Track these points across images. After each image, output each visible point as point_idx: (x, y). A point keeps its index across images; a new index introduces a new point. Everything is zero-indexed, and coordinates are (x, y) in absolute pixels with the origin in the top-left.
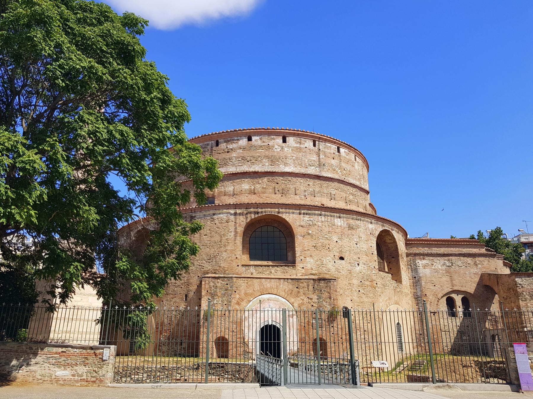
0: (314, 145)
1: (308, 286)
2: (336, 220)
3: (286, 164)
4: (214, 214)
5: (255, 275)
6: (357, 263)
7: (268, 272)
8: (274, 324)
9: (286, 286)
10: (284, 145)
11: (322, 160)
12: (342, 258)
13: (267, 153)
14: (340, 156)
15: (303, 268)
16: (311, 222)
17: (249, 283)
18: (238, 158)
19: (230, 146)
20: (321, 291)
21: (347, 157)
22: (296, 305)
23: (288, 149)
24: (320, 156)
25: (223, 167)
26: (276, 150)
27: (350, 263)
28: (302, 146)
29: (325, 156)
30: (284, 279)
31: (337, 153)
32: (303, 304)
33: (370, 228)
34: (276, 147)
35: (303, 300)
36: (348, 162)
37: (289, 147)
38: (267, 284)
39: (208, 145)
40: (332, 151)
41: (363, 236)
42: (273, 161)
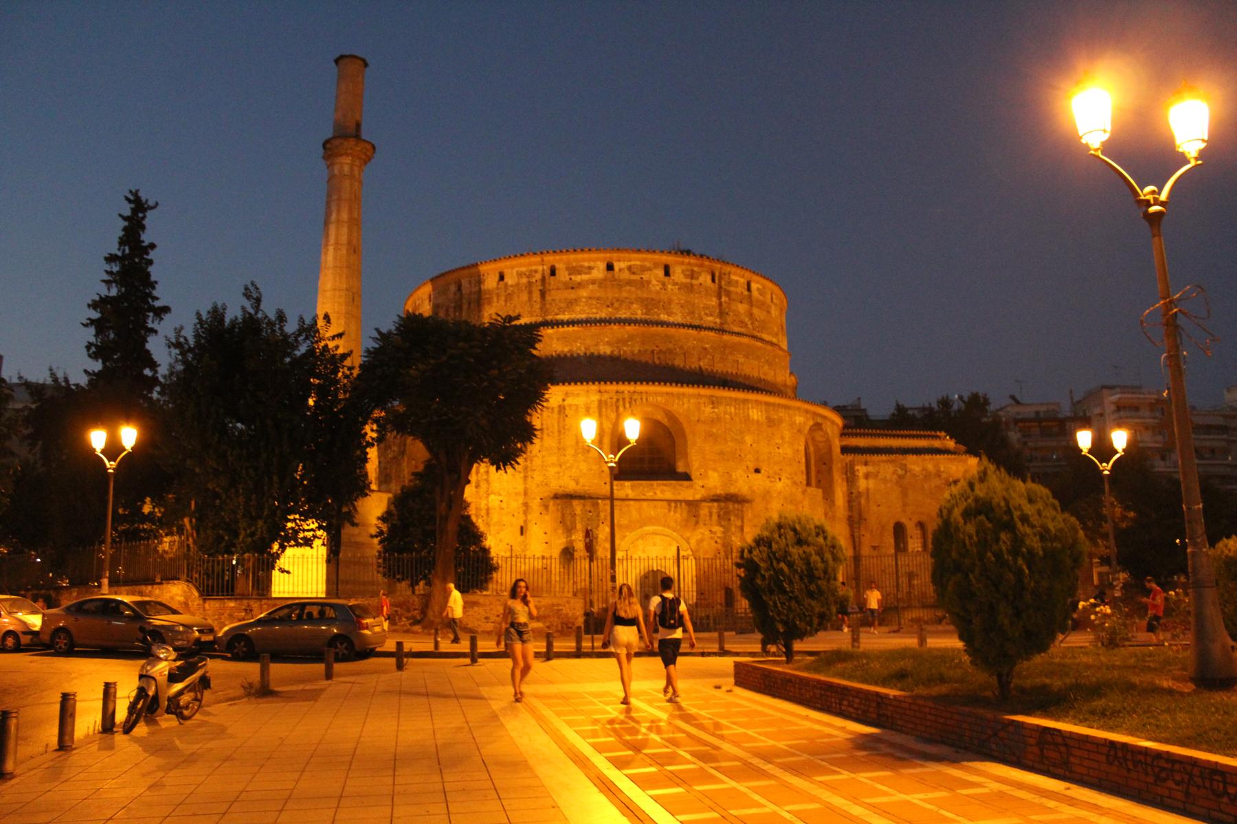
0: (713, 280)
1: (711, 514)
2: (750, 411)
3: (669, 314)
4: (564, 400)
5: (631, 497)
6: (777, 477)
7: (651, 494)
8: (659, 568)
9: (678, 515)
10: (666, 279)
11: (724, 305)
12: (757, 471)
13: (639, 293)
14: (750, 297)
15: (703, 486)
16: (714, 416)
17: (625, 509)
18: (590, 298)
19: (578, 278)
20: (729, 520)
21: (761, 298)
22: (693, 542)
23: (673, 287)
24: (719, 297)
25: (564, 314)
26: (653, 288)
27: (768, 477)
28: (694, 282)
29: (730, 299)
30: (676, 501)
31: (746, 293)
32: (701, 541)
33: (797, 422)
34: (654, 282)
35: (703, 534)
36: (762, 305)
37: (675, 284)
38: (649, 510)
39: (536, 271)
40: (739, 290)
41: (787, 434)
42: (648, 304)
